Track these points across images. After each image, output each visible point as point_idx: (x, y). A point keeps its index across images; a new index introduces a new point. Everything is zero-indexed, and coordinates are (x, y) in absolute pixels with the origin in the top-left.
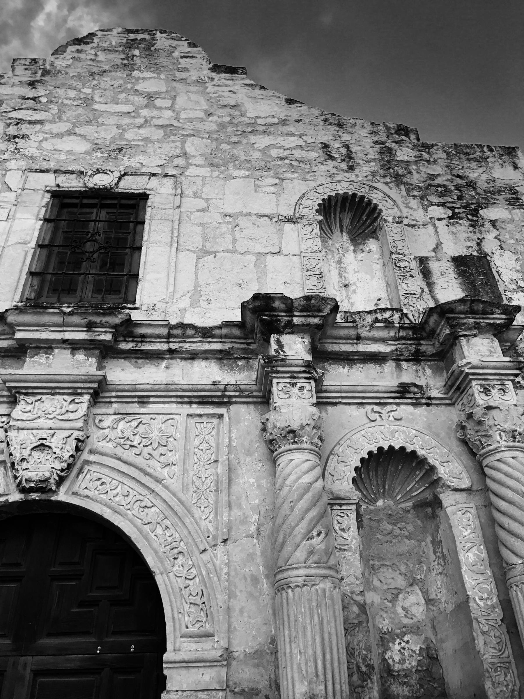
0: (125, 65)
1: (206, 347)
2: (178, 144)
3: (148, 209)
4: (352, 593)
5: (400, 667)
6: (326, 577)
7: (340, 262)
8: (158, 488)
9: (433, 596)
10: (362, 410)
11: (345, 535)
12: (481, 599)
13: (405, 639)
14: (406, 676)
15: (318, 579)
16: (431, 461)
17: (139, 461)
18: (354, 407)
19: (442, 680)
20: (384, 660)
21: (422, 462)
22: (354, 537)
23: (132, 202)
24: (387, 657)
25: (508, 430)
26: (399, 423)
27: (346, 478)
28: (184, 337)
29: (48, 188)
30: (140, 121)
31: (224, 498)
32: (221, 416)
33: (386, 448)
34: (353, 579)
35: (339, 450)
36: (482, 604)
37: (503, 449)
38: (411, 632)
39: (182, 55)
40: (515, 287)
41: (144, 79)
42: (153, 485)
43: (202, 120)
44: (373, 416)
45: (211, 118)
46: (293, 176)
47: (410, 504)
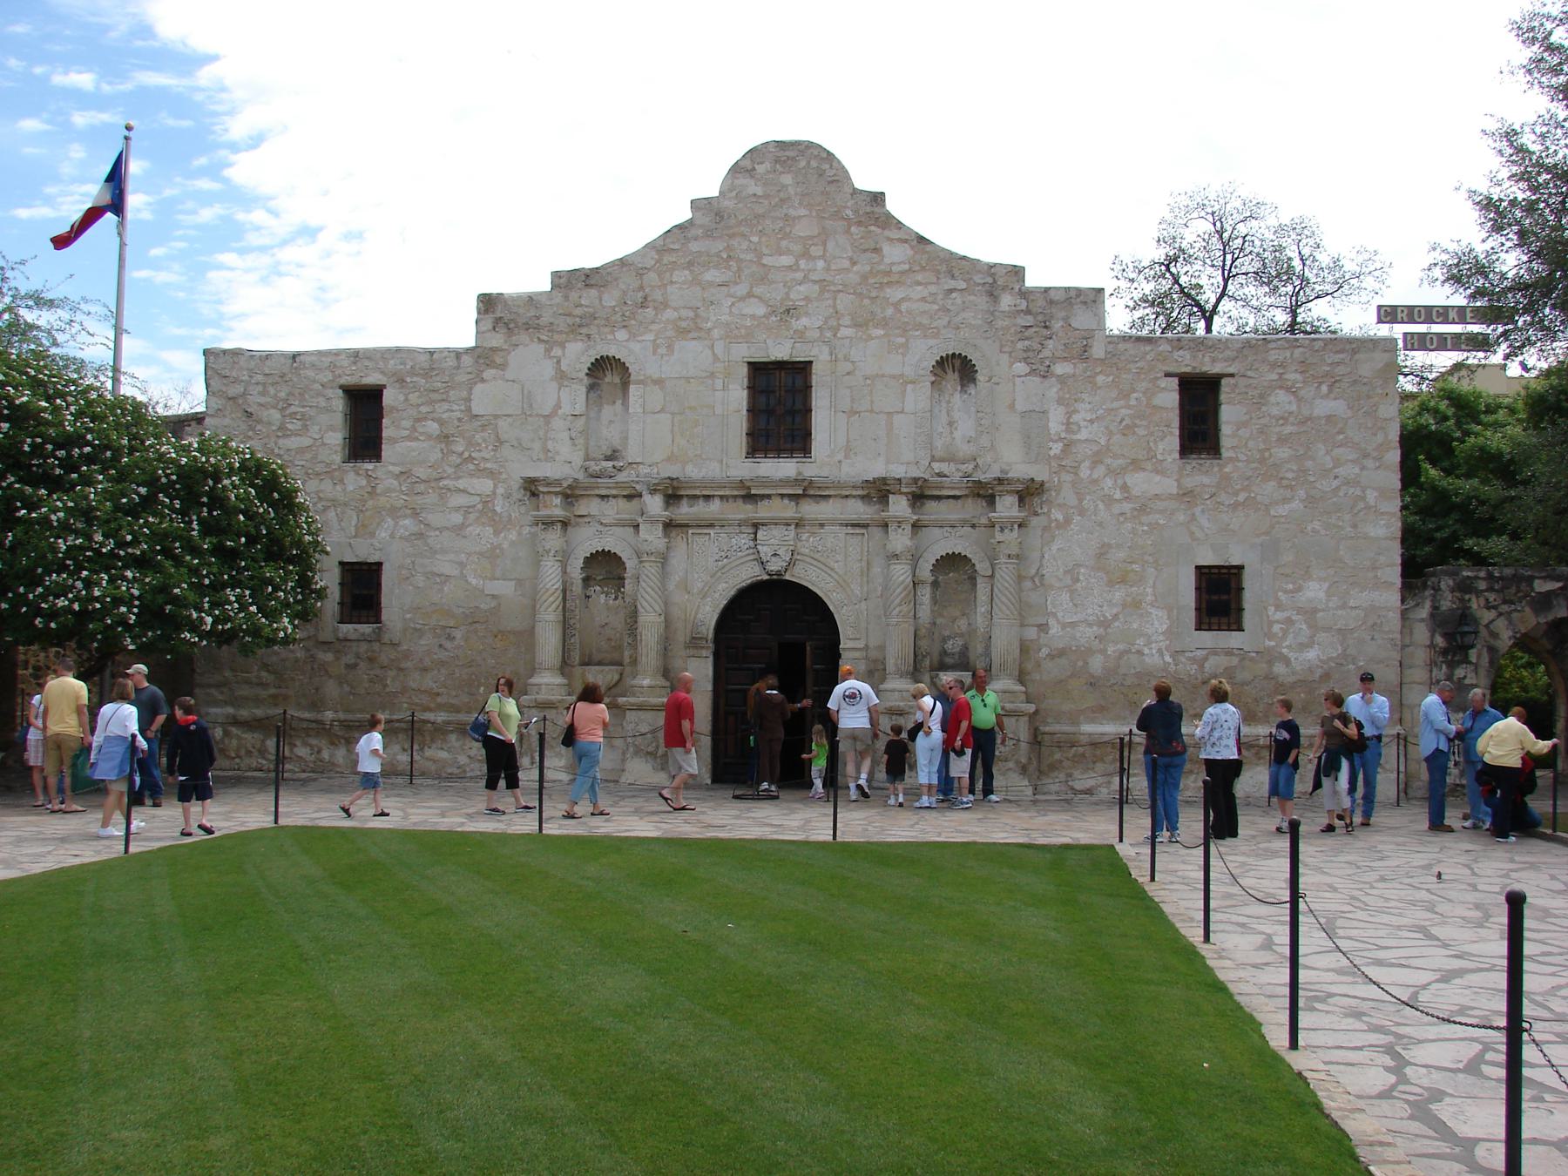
0: (781, 200)
1: (854, 493)
2: (830, 302)
3: (814, 377)
7: (949, 402)
8: (833, 574)
10: (941, 529)
17: (822, 559)
23: (802, 366)
28: (842, 488)
29: (745, 360)
30: (799, 275)
31: (865, 579)
35: (925, 554)
39: (830, 179)
40: (1056, 438)
41: (800, 217)
42: (829, 572)
43: (847, 270)
45: (855, 268)
46: (917, 333)
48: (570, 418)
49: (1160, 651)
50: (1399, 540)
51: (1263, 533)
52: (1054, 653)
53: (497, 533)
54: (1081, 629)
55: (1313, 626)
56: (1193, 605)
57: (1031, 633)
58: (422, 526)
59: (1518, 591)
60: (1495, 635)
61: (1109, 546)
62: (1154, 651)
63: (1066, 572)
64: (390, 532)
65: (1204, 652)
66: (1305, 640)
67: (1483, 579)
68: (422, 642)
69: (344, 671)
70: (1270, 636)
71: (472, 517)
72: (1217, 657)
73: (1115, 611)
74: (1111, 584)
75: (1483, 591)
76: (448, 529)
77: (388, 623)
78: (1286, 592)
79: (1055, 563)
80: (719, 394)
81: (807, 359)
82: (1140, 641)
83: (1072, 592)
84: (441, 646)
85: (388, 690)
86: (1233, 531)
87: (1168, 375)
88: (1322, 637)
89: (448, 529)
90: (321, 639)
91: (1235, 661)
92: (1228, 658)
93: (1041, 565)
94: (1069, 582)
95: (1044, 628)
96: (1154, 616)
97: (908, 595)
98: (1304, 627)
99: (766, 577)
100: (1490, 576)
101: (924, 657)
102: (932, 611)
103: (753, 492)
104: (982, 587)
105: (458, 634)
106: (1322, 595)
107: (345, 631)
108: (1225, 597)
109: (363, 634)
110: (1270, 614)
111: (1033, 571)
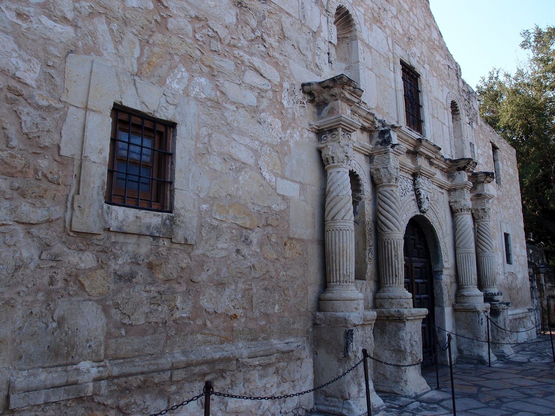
17: (433, 204)
48: (327, 43)
53: (284, 128)
58: (218, 93)
64: (183, 86)
68: (220, 246)
69: (112, 287)
71: (265, 103)
76: (244, 107)
77: (182, 212)
80: (392, 73)
81: (419, 73)
84: (238, 251)
85: (177, 315)
87: (491, 142)
89: (244, 107)
90: (77, 227)
99: (419, 213)
103: (421, 149)
105: (255, 237)
107: (121, 217)
109: (148, 228)
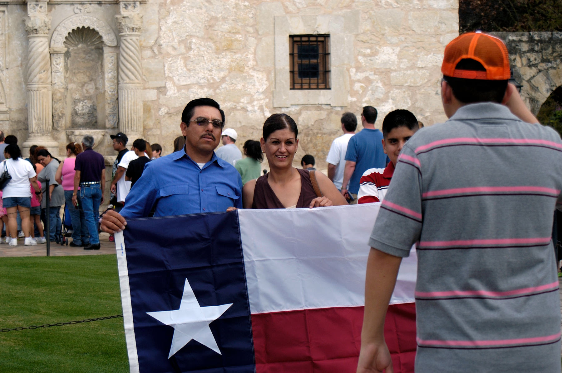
4: (59, 88)
5: (81, 112)
6: (45, 87)
9: (98, 86)
10: (72, 7)
11: (58, 66)
12: (110, 91)
13: (85, 102)
14: (83, 115)
15: (42, 89)
16: (100, 34)
18: (69, 5)
19: (96, 117)
20: (74, 109)
21: (98, 33)
22: (62, 67)
24: (76, 108)
25: (131, 27)
26: (88, 14)
27: (60, 42)
32: (4, 12)
33: (81, 27)
34: (60, 83)
35: (59, 29)
36: (109, 92)
37: (127, 35)
38: (88, 99)
44: (78, 11)
47: (93, 47)
49: (261, 108)
50: (457, 11)
51: (346, 7)
52: (172, 111)
54: (194, 90)
55: (389, 85)
56: (287, 68)
57: (152, 95)
59: (553, 52)
60: (535, 88)
61: (216, 19)
62: (256, 108)
63: (180, 42)
65: (298, 108)
66: (382, 96)
67: (526, 42)
70: (353, 93)
72: (309, 112)
73: (222, 74)
74: (218, 51)
75: (525, 52)
78: (365, 56)
79: (170, 35)
82: (244, 100)
83: (186, 59)
86: (321, 5)
88: (395, 92)
91: (324, 115)
92: (318, 112)
93: (159, 37)
94: (182, 49)
95: (162, 90)
96: (256, 79)
97: (46, 64)
98: (380, 84)
100: (531, 40)
101: (60, 117)
102: (65, 78)
104: (108, 56)
106: (394, 58)
108: (314, 61)
110: (352, 74)
111: (152, 42)
